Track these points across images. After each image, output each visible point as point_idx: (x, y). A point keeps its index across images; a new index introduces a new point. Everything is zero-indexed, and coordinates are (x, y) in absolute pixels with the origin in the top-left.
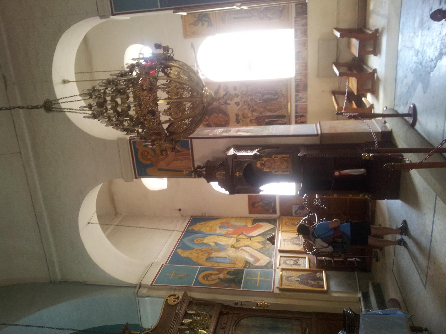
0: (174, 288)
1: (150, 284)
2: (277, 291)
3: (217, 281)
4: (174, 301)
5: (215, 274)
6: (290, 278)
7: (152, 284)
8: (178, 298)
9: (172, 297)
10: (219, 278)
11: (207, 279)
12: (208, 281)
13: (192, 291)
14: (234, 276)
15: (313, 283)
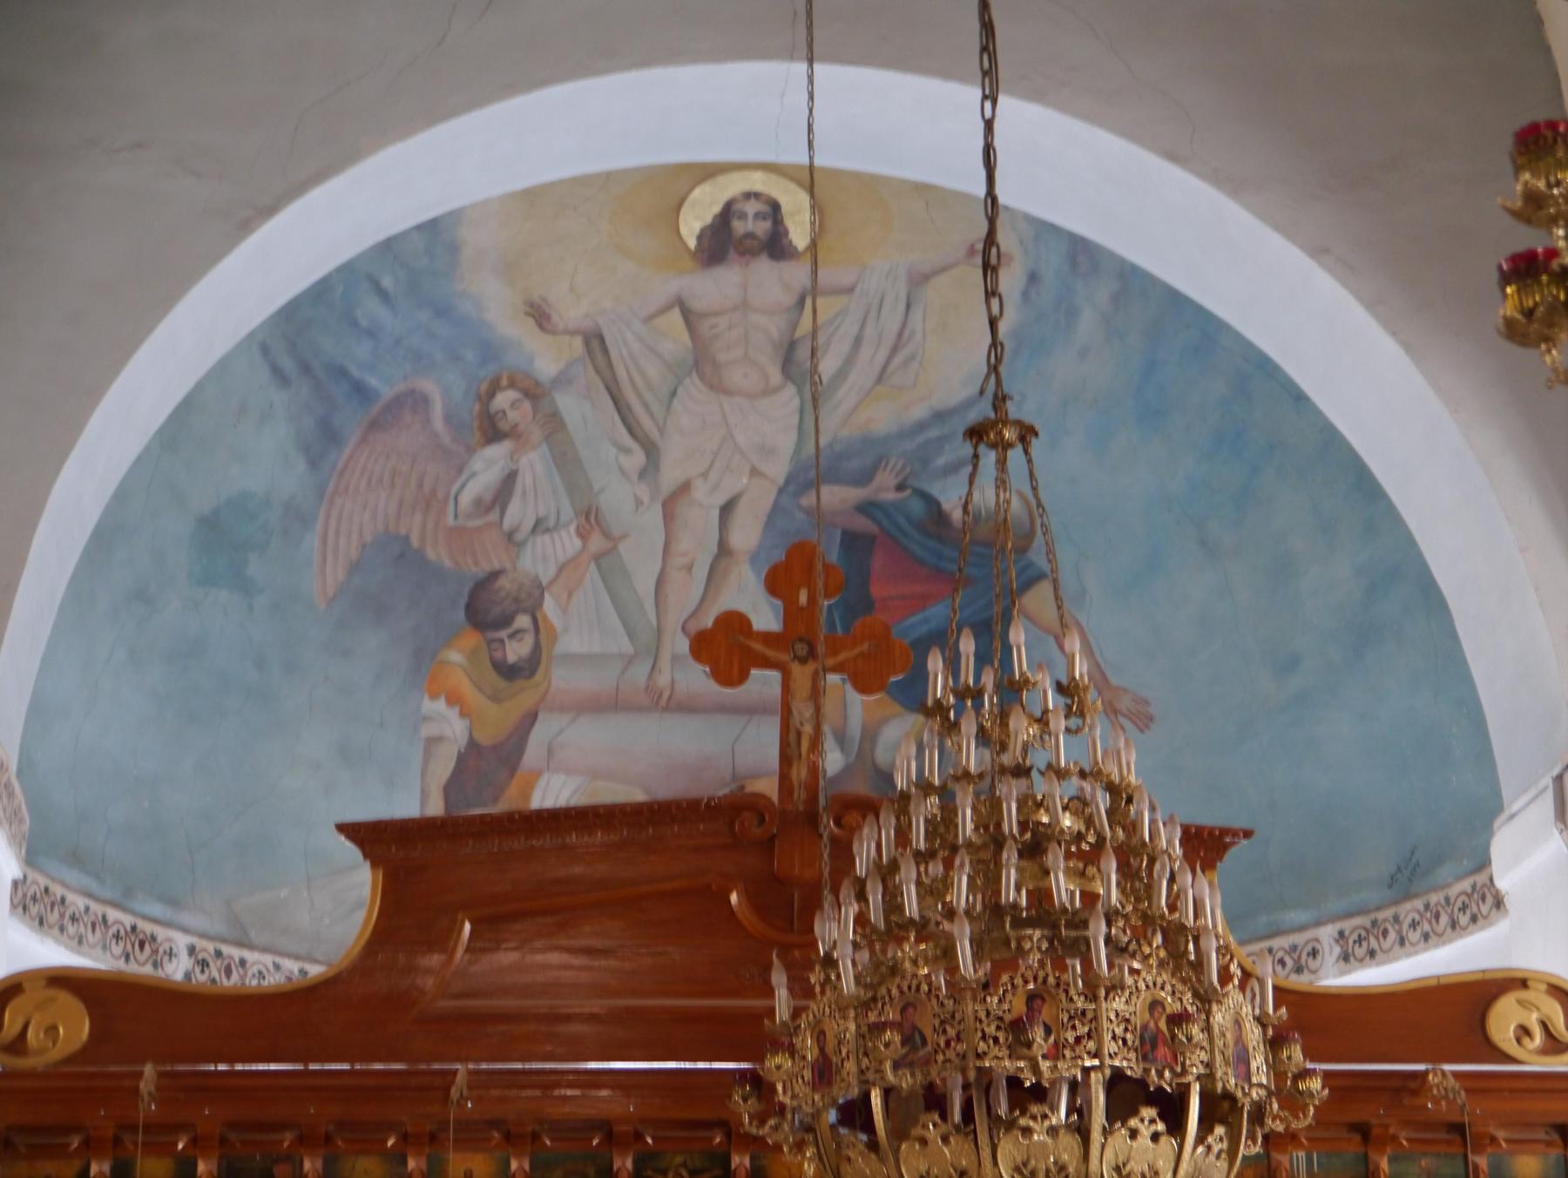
4: (1524, 1031)
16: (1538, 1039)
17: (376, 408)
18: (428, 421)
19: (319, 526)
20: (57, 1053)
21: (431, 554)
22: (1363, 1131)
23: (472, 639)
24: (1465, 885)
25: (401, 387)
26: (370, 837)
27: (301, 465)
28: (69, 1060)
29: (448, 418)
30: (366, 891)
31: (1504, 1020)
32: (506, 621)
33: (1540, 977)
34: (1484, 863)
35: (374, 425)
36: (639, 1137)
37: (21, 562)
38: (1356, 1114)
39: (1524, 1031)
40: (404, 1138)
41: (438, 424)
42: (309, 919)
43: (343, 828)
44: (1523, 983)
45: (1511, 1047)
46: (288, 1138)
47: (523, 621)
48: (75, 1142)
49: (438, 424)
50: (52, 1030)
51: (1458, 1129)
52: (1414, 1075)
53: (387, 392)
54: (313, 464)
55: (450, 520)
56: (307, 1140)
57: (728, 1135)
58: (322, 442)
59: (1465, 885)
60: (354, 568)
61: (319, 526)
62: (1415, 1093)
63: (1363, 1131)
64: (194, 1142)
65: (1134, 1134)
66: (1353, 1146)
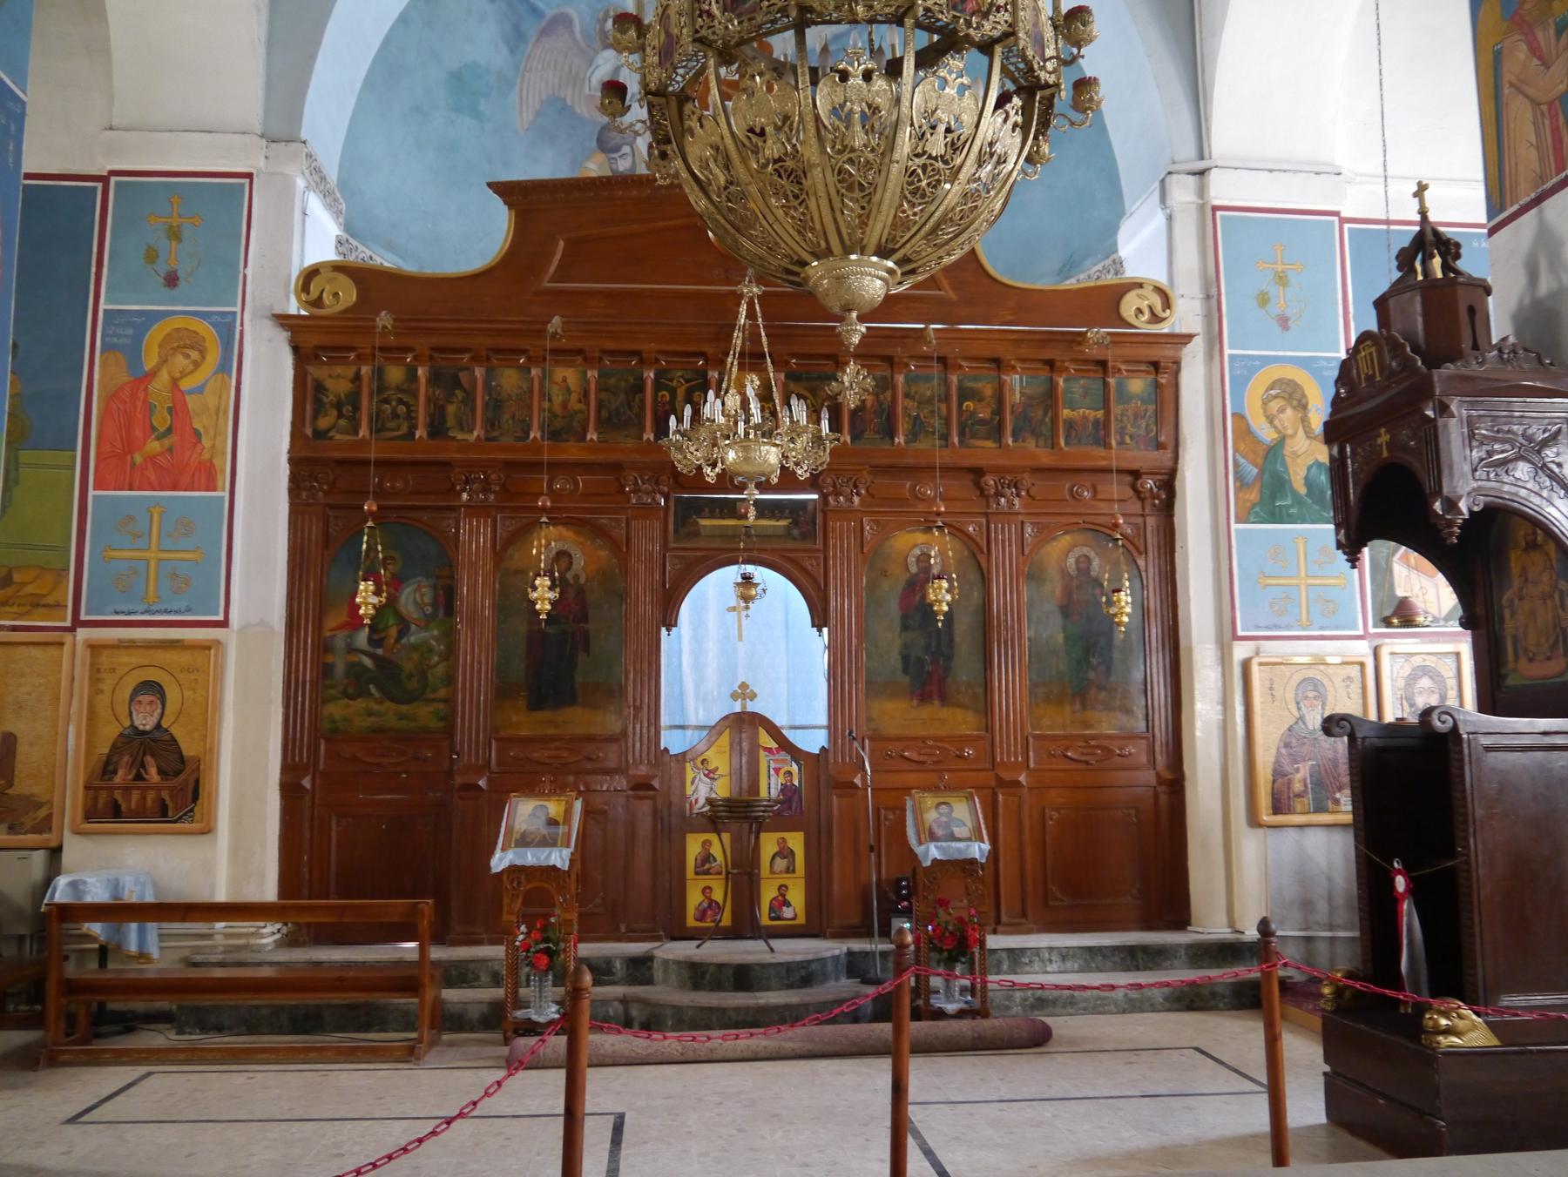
0: (1214, 291)
1: (1217, 203)
2: (1240, 651)
3: (1267, 434)
4: (1140, 311)
5: (1304, 420)
6: (1311, 694)
7: (1215, 209)
8: (1156, 319)
9: (1157, 302)
10: (1282, 440)
11: (1276, 397)
12: (1265, 404)
13: (1209, 357)
14: (1303, 491)
15: (1299, 776)
16: (1147, 316)
17: (544, 22)
18: (572, 32)
19: (517, 88)
20: (339, 308)
21: (577, 110)
22: (1050, 364)
23: (601, 157)
24: (1099, 267)
25: (556, 11)
26: (504, 190)
27: (504, 51)
28: (346, 311)
29: (583, 32)
30: (505, 225)
31: (1129, 305)
32: (617, 149)
33: (1149, 282)
34: (1114, 249)
35: (545, 32)
36: (657, 361)
37: (319, 44)
38: (1048, 354)
39: (1140, 311)
40: (529, 359)
41: (578, 35)
42: (474, 237)
43: (490, 185)
44: (1140, 286)
45: (1133, 320)
46: (466, 357)
47: (626, 149)
48: (352, 355)
49: (578, 35)
50: (336, 295)
51: (1103, 364)
52: (1080, 334)
53: (550, 13)
54: (512, 51)
55: (587, 92)
56: (476, 359)
57: (706, 361)
58: (515, 38)
59: (1099, 267)
60: (538, 114)
61: (517, 88)
62: (1080, 343)
63: (1050, 364)
64: (415, 358)
65: (945, 82)
66: (1044, 373)
